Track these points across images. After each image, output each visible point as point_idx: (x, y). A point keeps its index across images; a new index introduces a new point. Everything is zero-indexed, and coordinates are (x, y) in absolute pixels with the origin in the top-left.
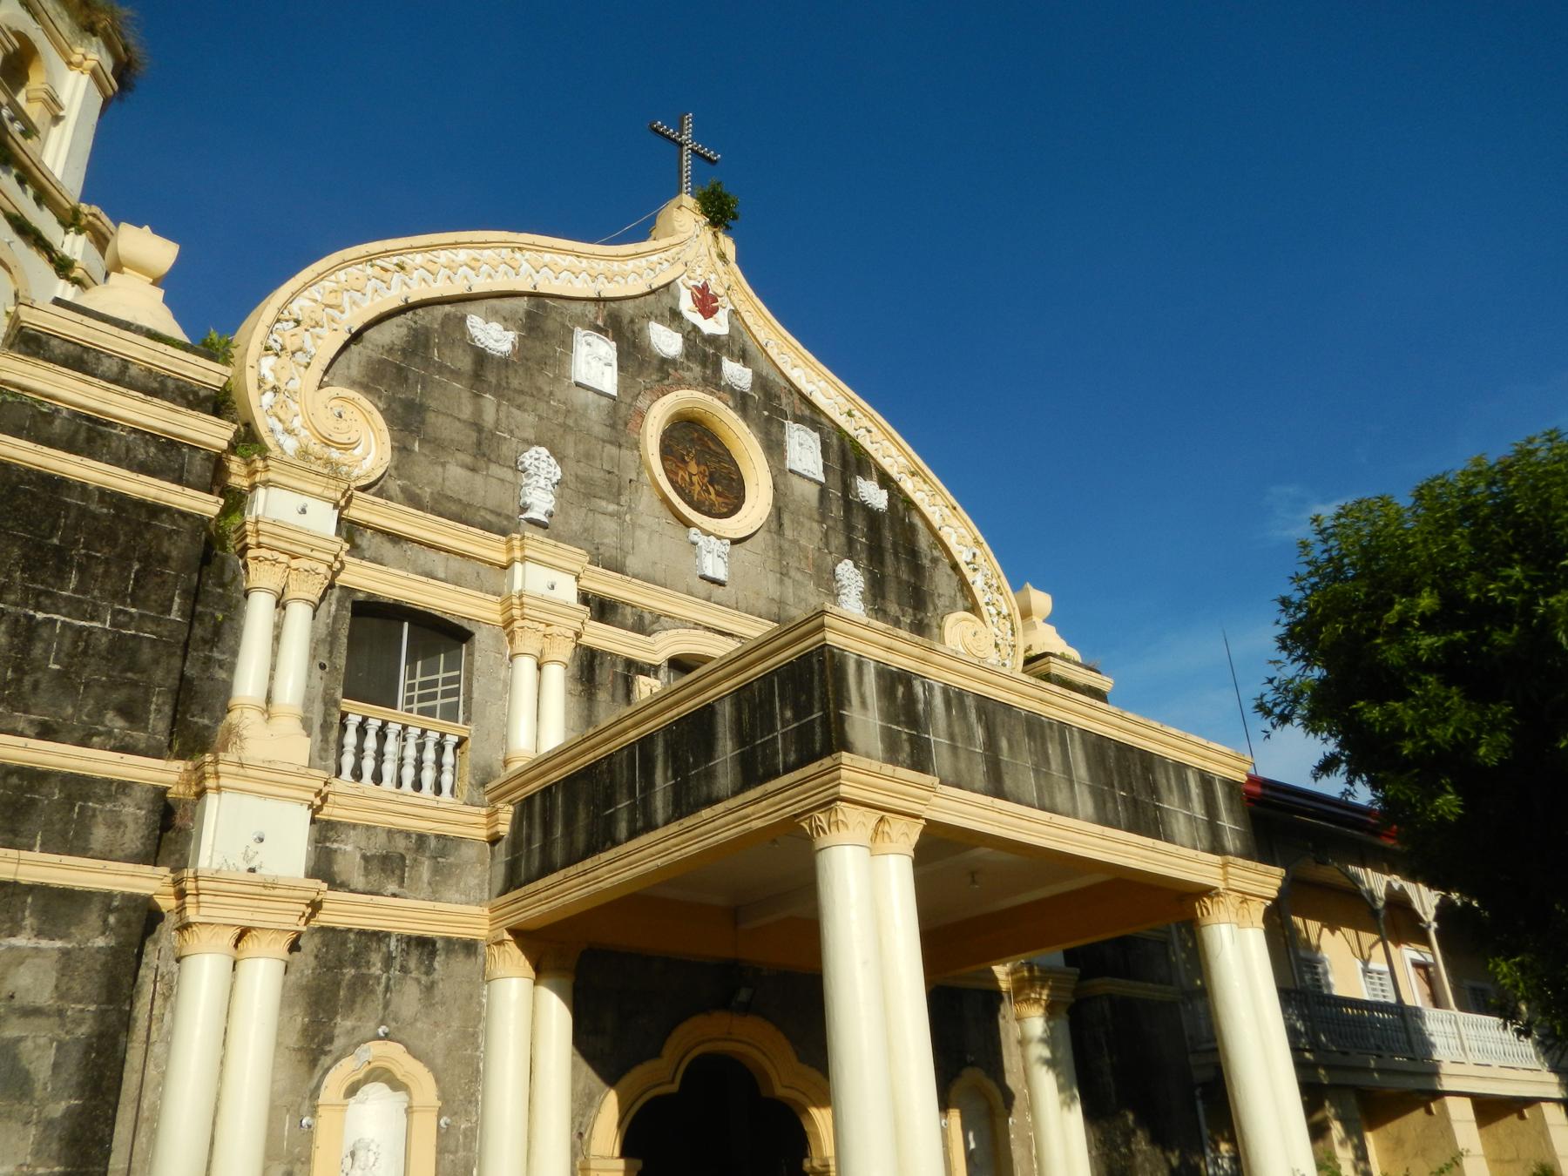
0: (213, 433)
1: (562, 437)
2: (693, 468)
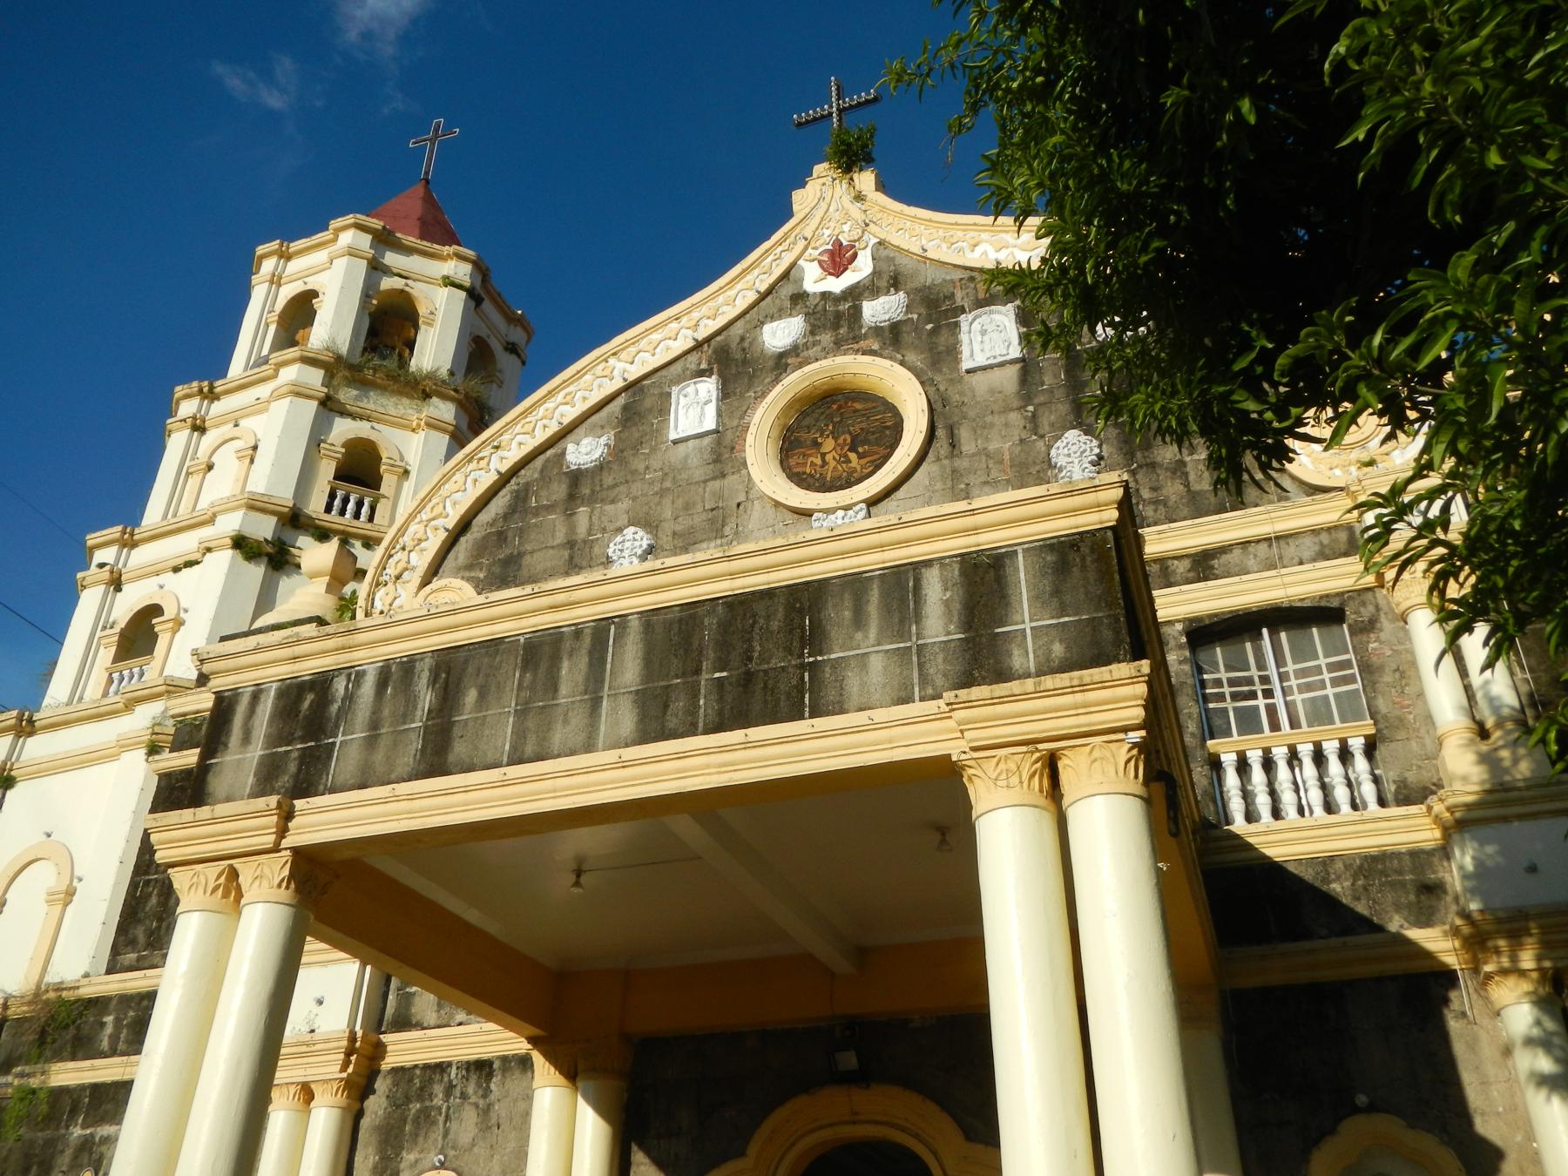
1: (659, 503)
2: (828, 445)
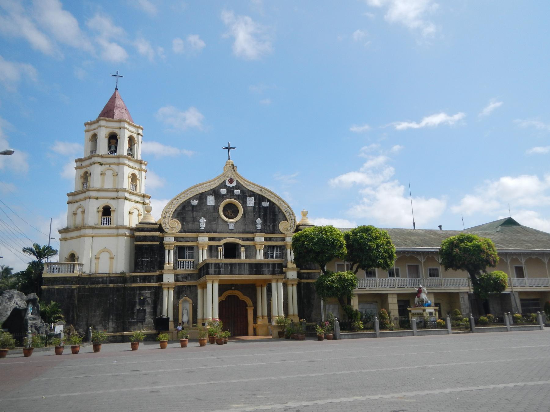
0: (157, 234)
2: (229, 211)
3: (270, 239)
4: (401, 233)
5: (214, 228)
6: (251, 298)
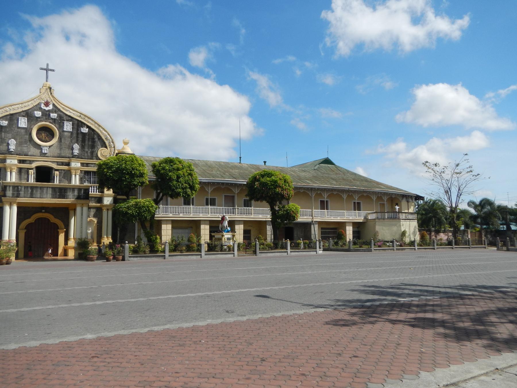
2: (43, 135)
3: (87, 165)
4: (208, 166)
5: (26, 150)
6: (63, 221)
